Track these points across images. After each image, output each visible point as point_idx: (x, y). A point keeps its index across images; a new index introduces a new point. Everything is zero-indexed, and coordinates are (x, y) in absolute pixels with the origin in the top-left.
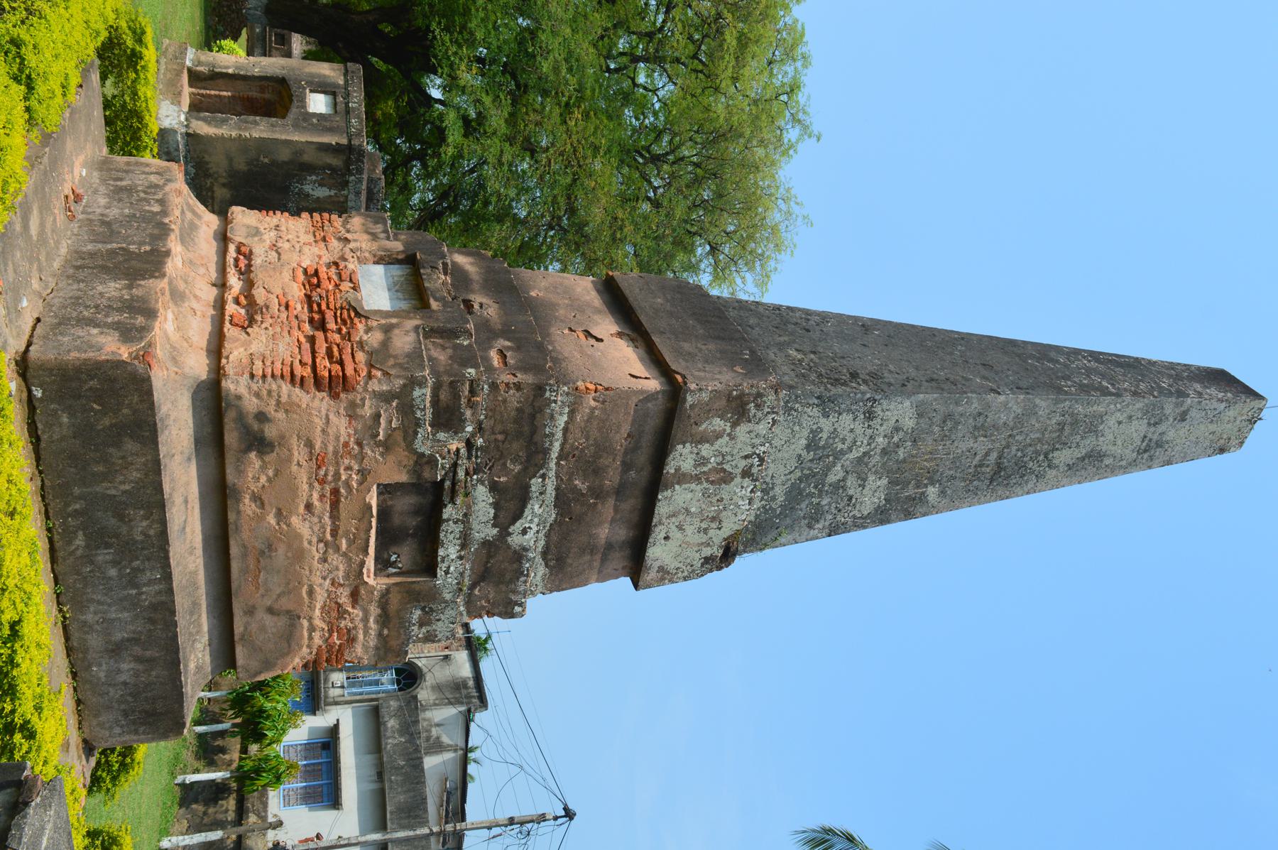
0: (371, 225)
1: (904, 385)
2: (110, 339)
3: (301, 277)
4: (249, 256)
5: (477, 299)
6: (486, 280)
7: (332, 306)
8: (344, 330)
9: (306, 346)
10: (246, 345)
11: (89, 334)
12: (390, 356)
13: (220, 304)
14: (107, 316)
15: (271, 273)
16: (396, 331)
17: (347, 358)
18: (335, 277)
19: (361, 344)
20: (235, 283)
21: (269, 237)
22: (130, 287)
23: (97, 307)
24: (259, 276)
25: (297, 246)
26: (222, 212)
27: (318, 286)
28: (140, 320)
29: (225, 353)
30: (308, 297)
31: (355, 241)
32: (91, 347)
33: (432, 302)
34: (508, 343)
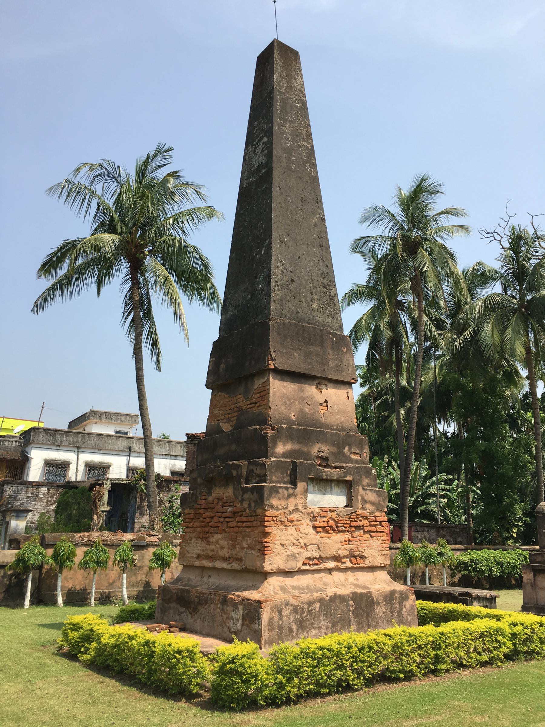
0: (281, 496)
1: (327, 266)
2: (407, 604)
3: (323, 534)
4: (309, 559)
5: (315, 450)
6: (300, 442)
7: (349, 522)
8: (360, 518)
9: (373, 534)
10: (374, 557)
11: (406, 611)
12: (379, 503)
13: (346, 570)
14: (396, 608)
15: (327, 548)
16: (366, 498)
17: (379, 519)
18: (325, 519)
19: (370, 513)
20: (331, 564)
21: (296, 550)
22: (378, 604)
23: (391, 612)
24: (330, 553)
25: (302, 535)
26: (266, 575)
27: (331, 527)
28: (397, 595)
29: (379, 565)
30: (340, 532)
31: (296, 505)
32: (412, 608)
33: (347, 479)
34: (346, 449)
